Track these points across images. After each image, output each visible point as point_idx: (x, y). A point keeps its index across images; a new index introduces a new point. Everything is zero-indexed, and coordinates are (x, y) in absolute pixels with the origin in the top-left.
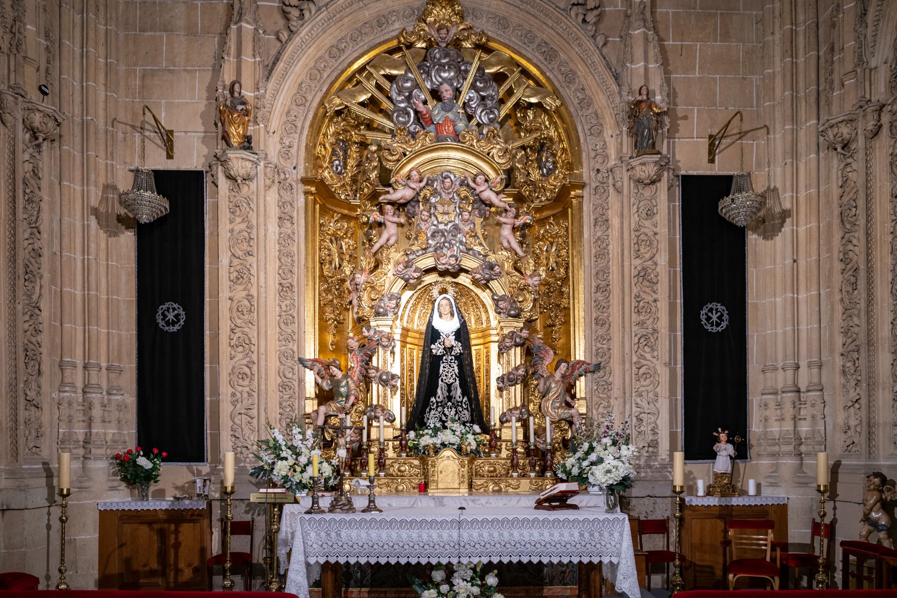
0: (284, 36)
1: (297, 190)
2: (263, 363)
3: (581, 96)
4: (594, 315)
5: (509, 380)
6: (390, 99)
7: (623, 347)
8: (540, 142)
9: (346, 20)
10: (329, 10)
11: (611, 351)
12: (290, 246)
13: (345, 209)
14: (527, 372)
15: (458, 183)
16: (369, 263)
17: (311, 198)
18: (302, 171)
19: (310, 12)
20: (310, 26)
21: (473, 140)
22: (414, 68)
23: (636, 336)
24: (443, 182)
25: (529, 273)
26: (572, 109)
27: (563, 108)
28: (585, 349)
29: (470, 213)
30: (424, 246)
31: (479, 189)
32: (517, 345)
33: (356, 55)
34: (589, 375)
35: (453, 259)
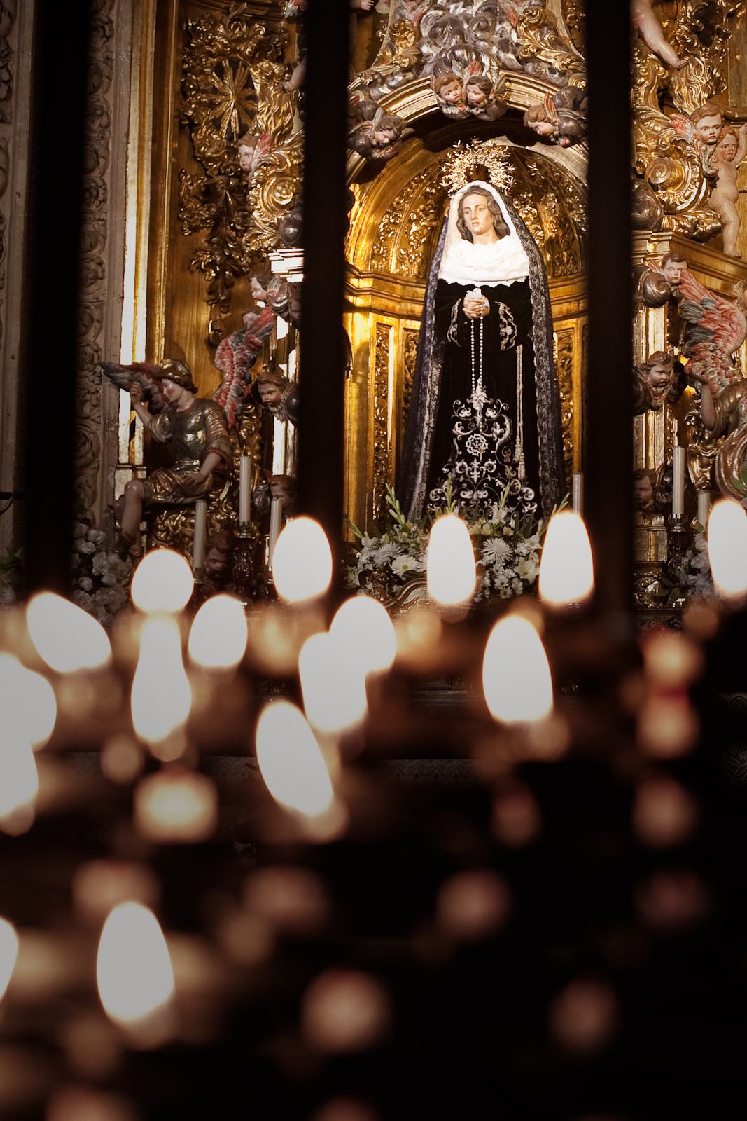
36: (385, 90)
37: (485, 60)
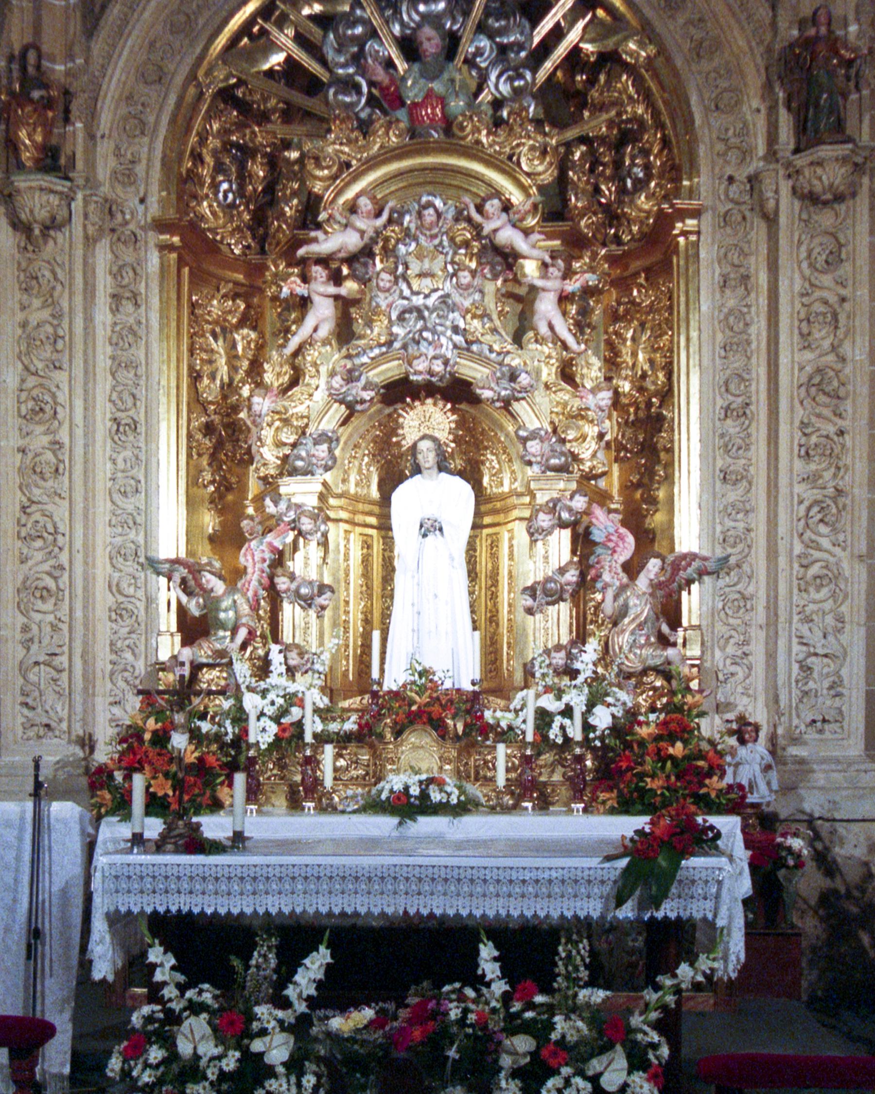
1: (146, 242)
2: (79, 569)
3: (698, 35)
4: (719, 463)
5: (547, 593)
6: (323, 61)
8: (620, 129)
11: (753, 534)
12: (133, 348)
13: (237, 271)
14: (583, 575)
18: (156, 206)
21: (479, 132)
23: (801, 502)
24: (420, 215)
25: (589, 385)
26: (679, 62)
27: (659, 62)
28: (701, 530)
29: (473, 273)
31: (488, 227)
32: (563, 525)
35: (439, 362)
36: (365, 359)
37: (443, 340)
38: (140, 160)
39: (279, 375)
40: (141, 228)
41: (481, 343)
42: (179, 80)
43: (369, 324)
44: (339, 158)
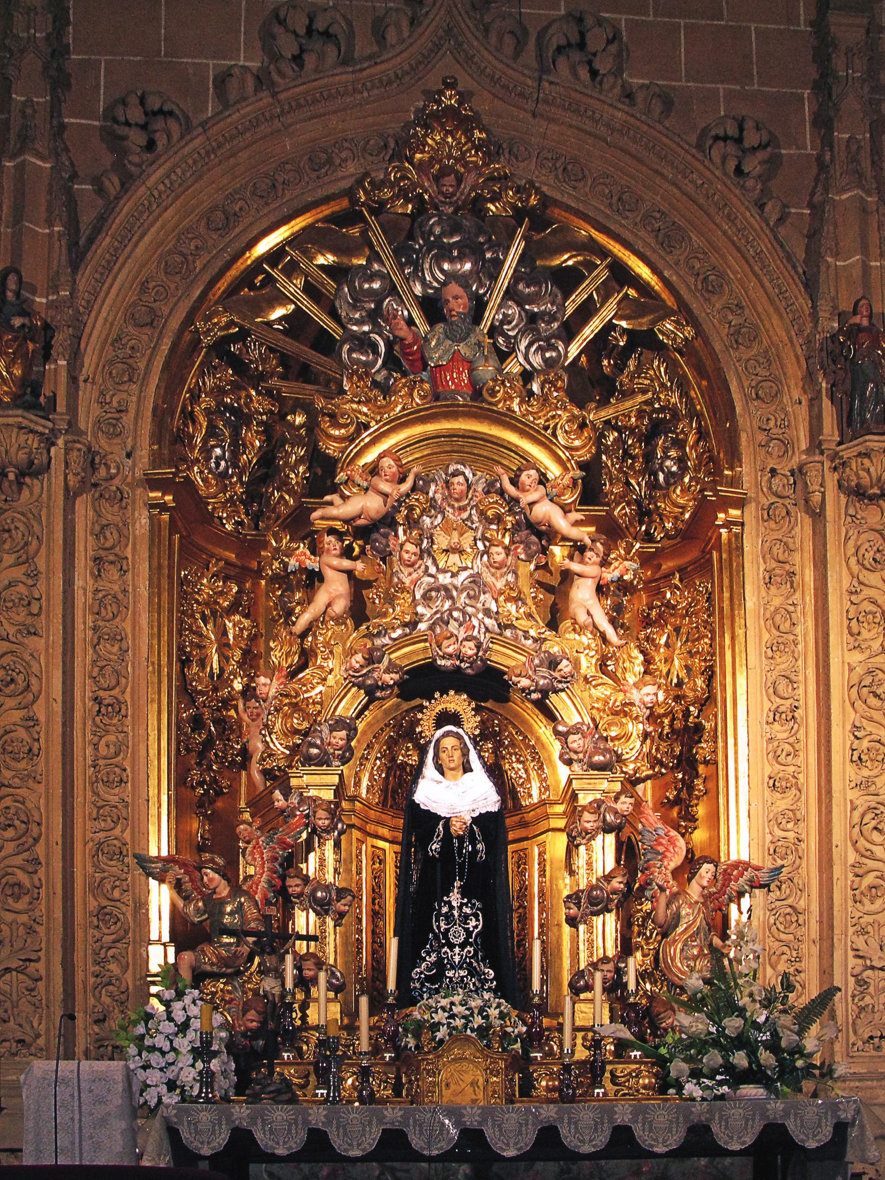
0: (112, 184)
7: (830, 832)
9: (243, 156)
10: (209, 134)
15: (480, 489)
16: (288, 655)
17: (166, 517)
19: (169, 137)
20: (168, 165)
21: (511, 399)
22: (385, 251)
30: (407, 618)
32: (607, 829)
33: (265, 224)
34: (757, 891)
36: (386, 640)
38: (127, 411)
39: (288, 655)
40: (128, 485)
41: (516, 628)
42: (175, 324)
43: (390, 600)
44: (357, 418)
